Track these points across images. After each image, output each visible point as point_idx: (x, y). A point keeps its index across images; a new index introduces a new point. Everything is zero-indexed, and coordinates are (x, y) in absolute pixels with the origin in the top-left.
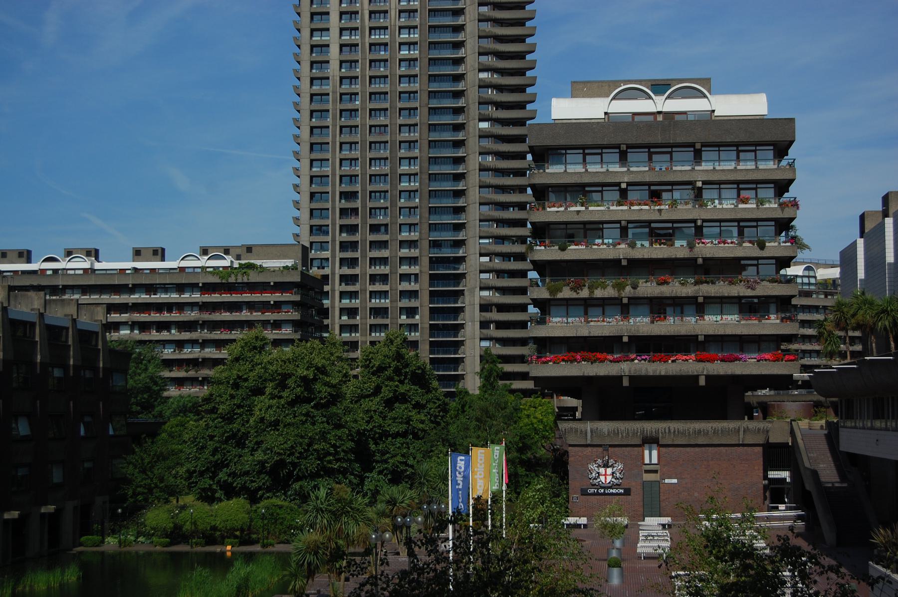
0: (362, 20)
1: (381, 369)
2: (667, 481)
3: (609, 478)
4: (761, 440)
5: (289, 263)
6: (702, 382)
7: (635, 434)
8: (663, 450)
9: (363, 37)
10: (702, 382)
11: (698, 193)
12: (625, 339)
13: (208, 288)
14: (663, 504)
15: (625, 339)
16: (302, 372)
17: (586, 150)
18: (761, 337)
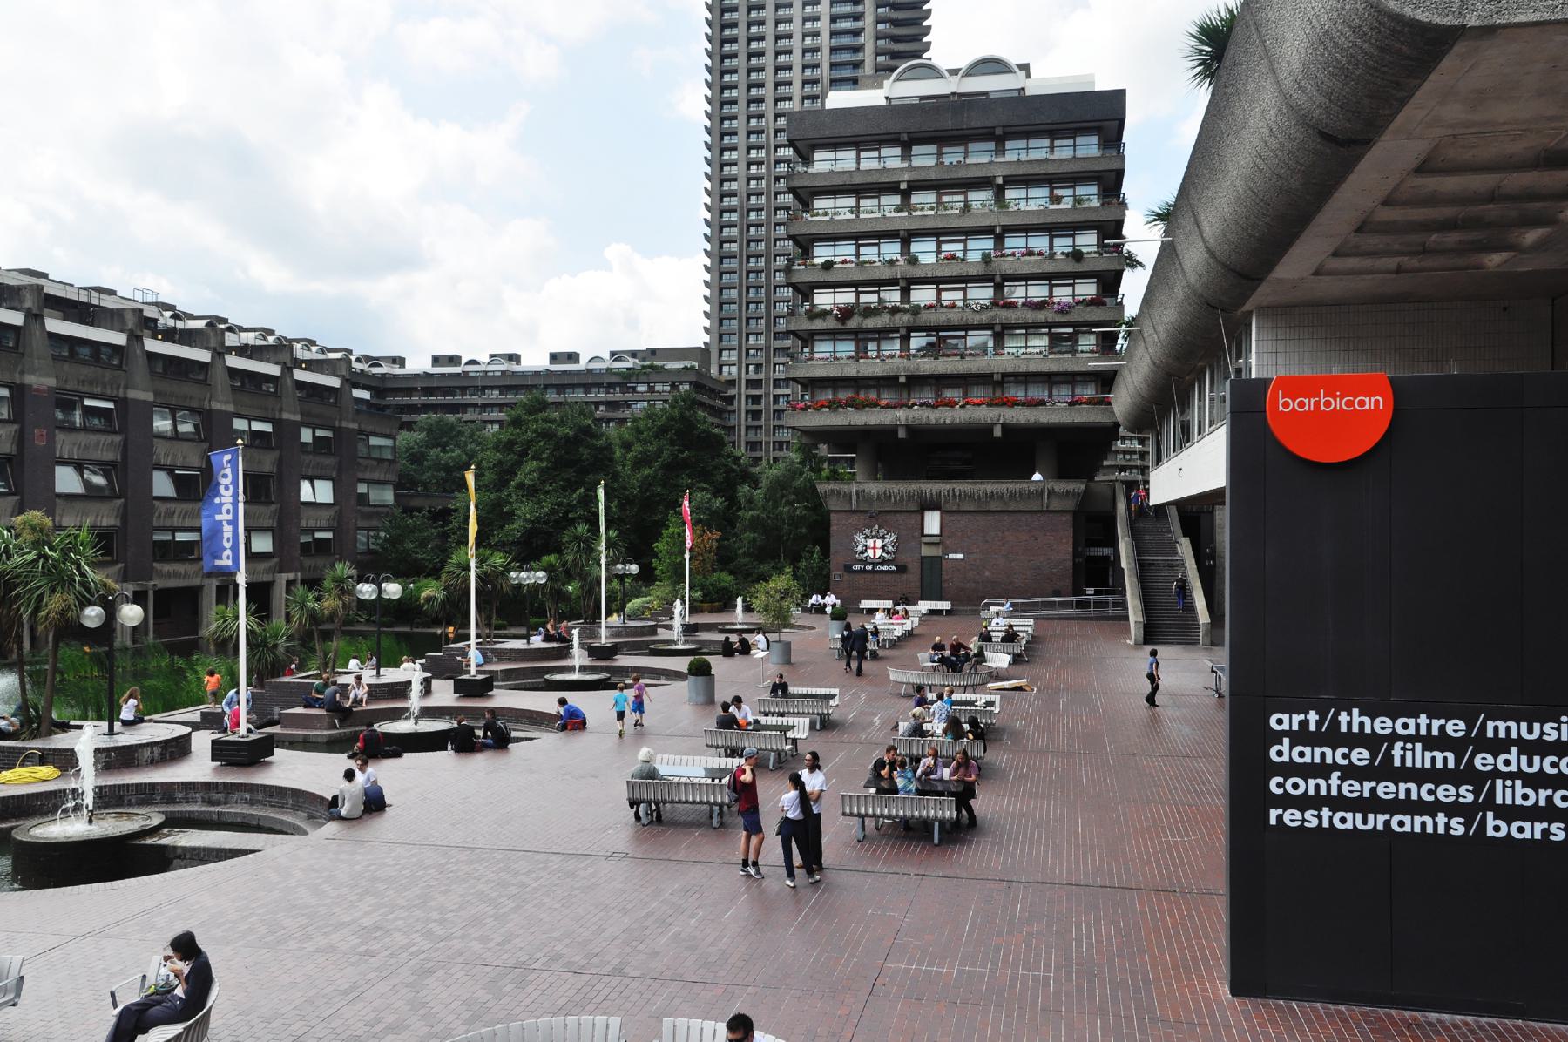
0: (768, 138)
1: (663, 430)
2: (951, 556)
3: (879, 552)
4: (1070, 504)
5: (688, 363)
6: (998, 432)
7: (910, 497)
8: (948, 517)
9: (768, 154)
10: (998, 432)
11: (999, 192)
12: (902, 380)
13: (611, 386)
14: (945, 585)
15: (902, 380)
16: (564, 431)
17: (859, 143)
18: (1075, 374)
